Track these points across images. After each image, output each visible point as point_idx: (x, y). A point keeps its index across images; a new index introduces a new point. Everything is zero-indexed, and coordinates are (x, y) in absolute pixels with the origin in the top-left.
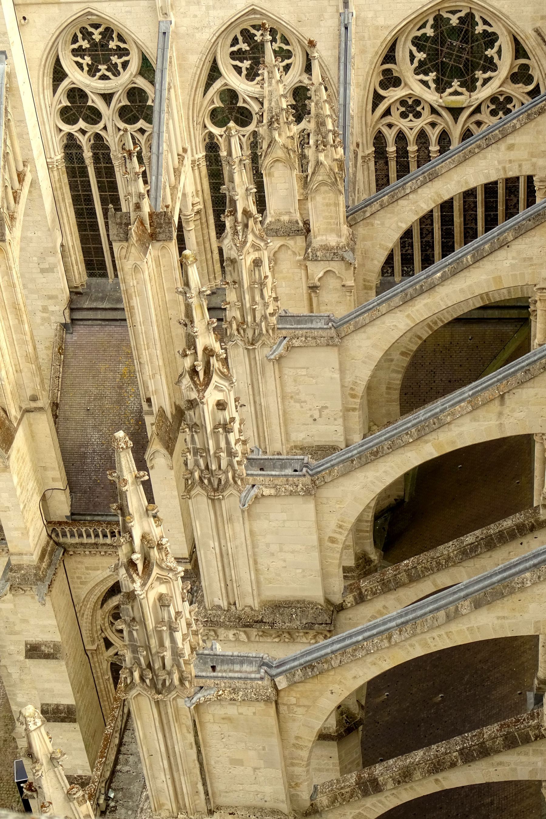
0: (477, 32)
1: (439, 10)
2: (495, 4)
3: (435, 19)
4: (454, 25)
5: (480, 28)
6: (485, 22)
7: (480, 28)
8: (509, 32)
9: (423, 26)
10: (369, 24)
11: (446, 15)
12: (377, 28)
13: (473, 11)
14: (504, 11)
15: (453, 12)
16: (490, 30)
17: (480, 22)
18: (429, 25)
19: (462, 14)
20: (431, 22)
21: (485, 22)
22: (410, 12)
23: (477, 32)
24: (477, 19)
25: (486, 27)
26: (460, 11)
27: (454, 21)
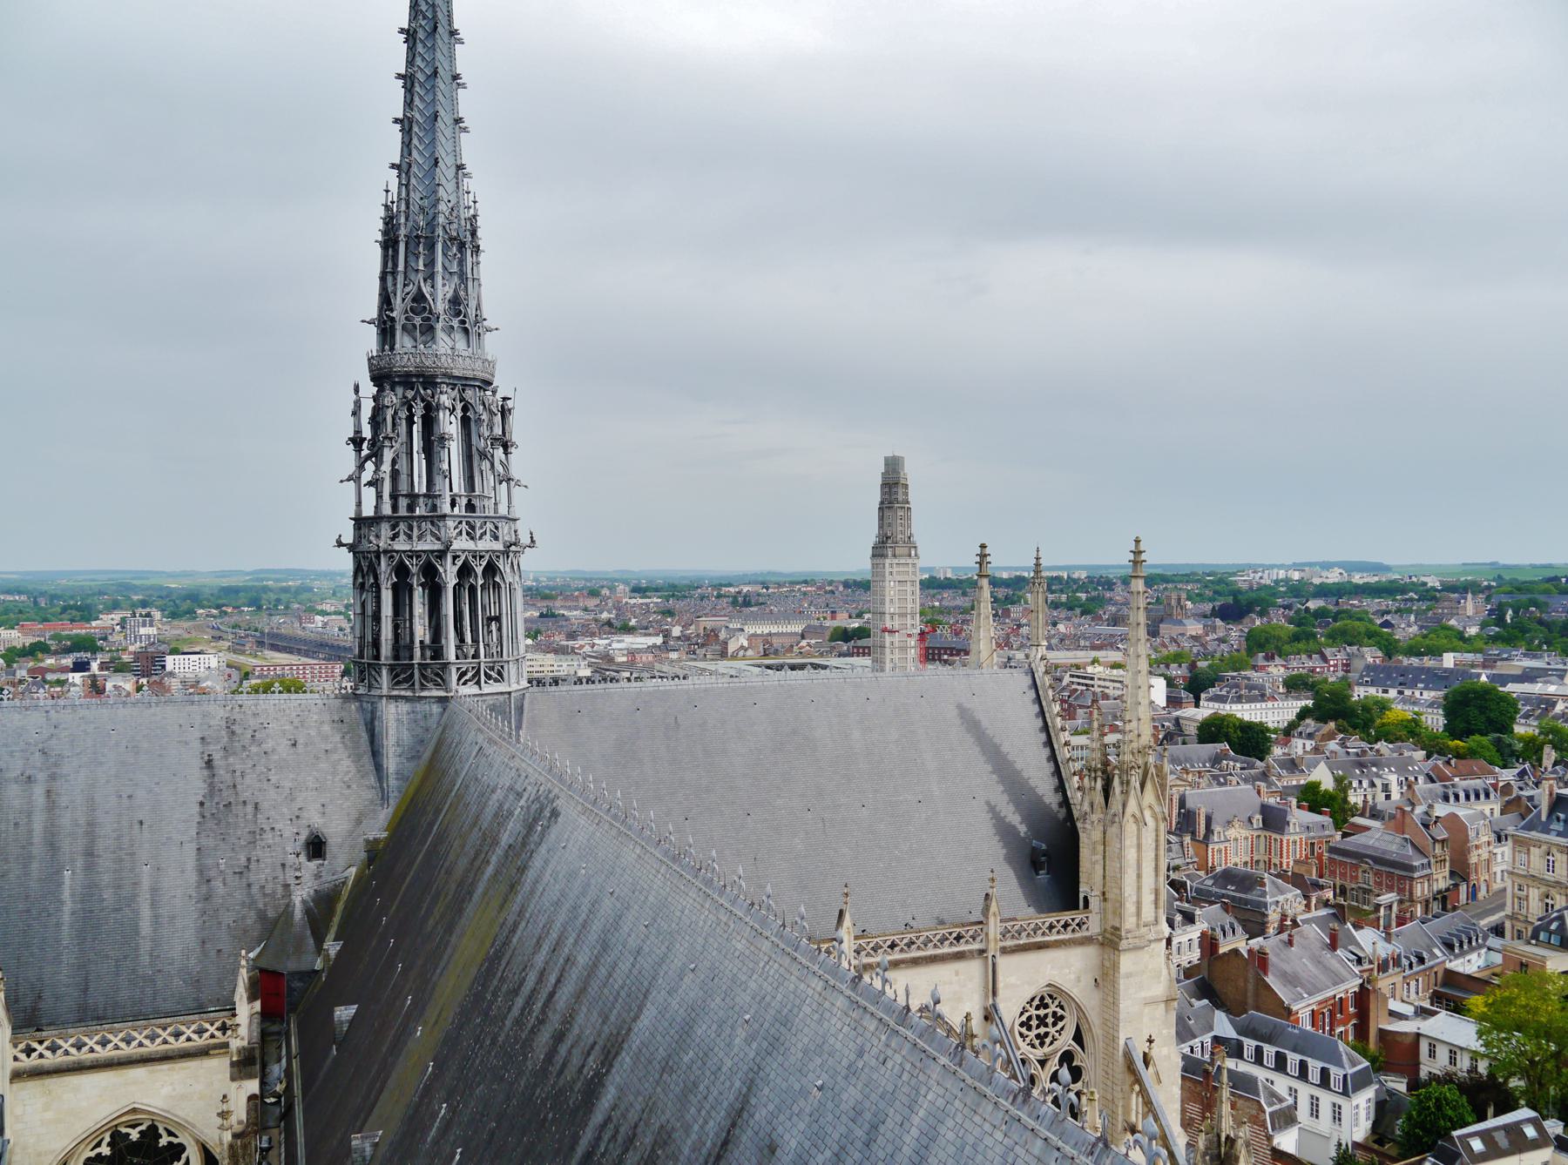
0: (160, 1145)
1: (116, 1126)
2: (180, 1113)
3: (112, 1136)
4: (135, 1140)
5: (164, 1141)
6: (170, 1133)
7: (164, 1141)
8: (197, 1141)
9: (98, 1145)
10: (30, 1151)
11: (124, 1130)
12: (39, 1155)
13: (156, 1123)
14: (189, 1119)
15: (134, 1127)
16: (175, 1141)
17: (164, 1134)
18: (104, 1144)
19: (143, 1128)
20: (107, 1139)
21: (170, 1133)
22: (80, 1132)
23: (160, 1145)
24: (161, 1131)
25: (171, 1139)
26: (141, 1124)
27: (134, 1135)
